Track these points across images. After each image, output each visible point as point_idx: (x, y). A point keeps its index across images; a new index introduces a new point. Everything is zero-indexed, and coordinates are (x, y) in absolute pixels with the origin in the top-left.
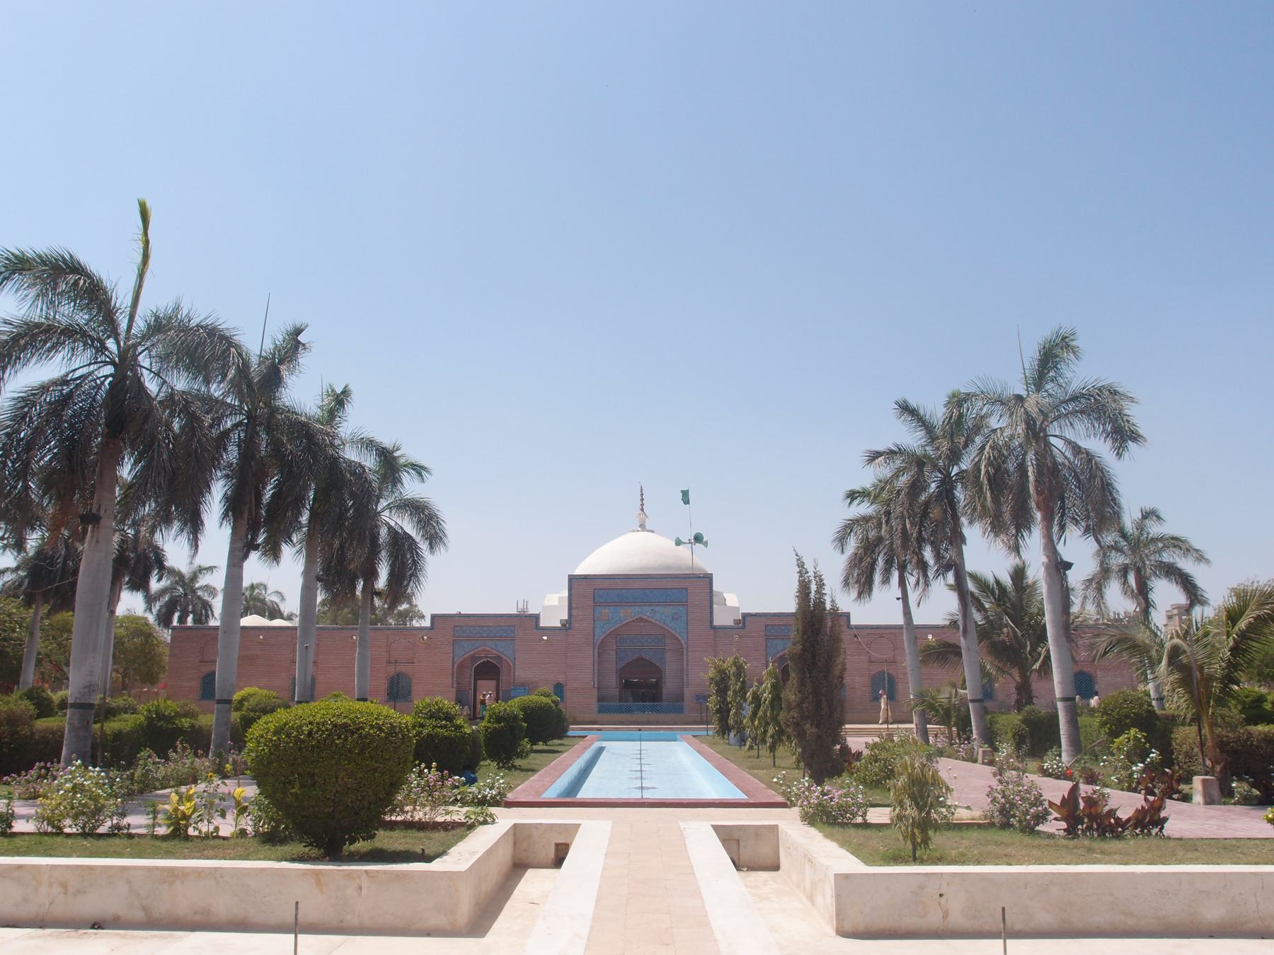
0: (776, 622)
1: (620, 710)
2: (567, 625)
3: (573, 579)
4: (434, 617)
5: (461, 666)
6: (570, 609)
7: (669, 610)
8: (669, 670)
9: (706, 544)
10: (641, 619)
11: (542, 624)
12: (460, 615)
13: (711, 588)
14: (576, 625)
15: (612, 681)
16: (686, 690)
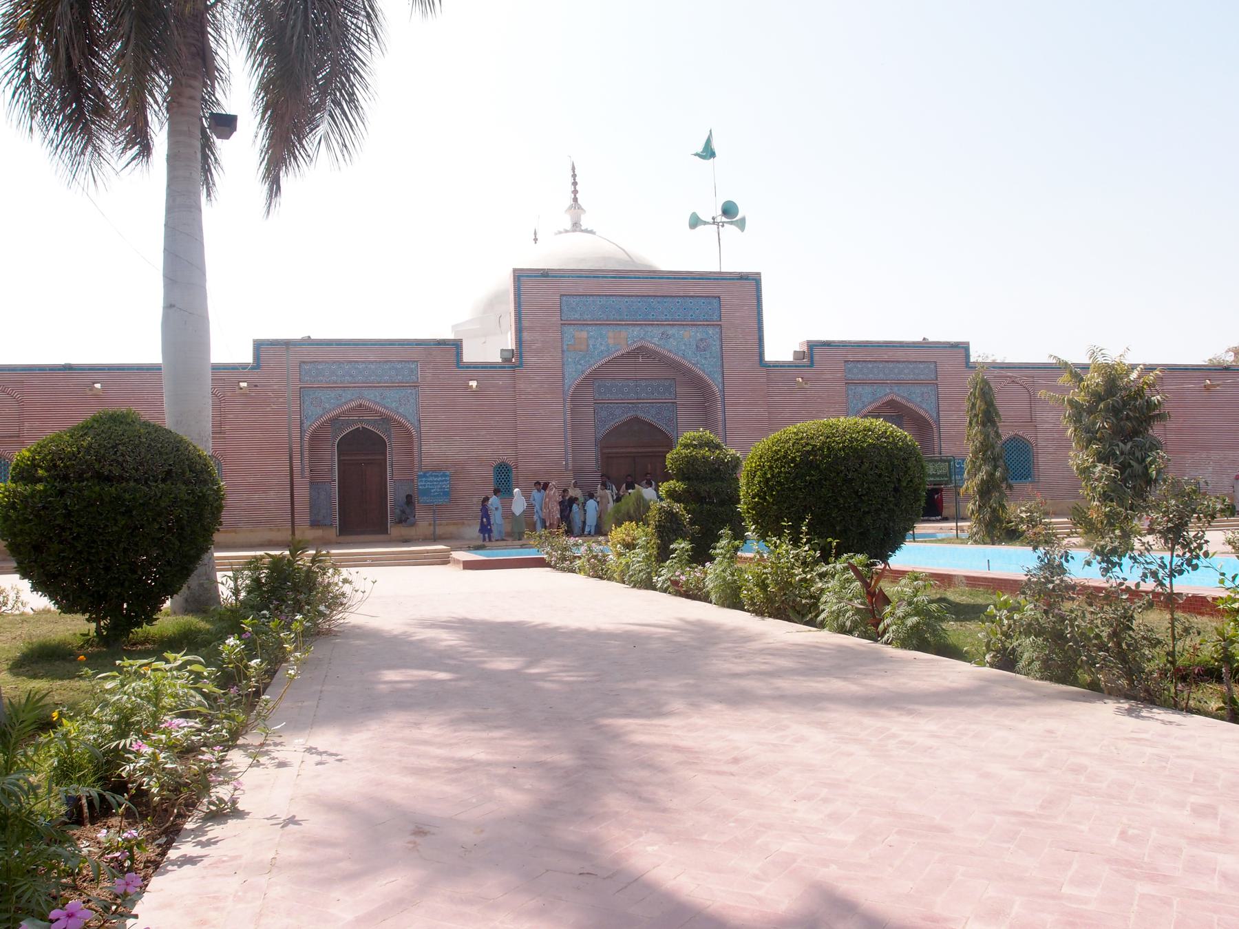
2: (513, 361)
3: (520, 276)
5: (315, 438)
6: (519, 331)
9: (741, 224)
10: (641, 352)
11: (469, 356)
12: (308, 342)
14: (530, 359)
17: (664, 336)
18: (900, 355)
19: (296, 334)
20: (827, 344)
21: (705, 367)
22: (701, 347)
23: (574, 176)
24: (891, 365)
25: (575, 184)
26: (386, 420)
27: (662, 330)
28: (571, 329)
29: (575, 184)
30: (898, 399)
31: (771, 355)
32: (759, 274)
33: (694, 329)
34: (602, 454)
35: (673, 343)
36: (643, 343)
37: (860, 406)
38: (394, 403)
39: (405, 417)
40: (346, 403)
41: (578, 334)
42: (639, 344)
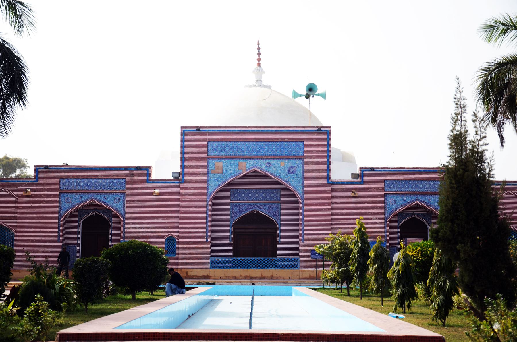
0: (396, 176)
1: (235, 265)
2: (179, 178)
3: (185, 131)
4: (38, 169)
5: (68, 219)
6: (183, 161)
7: (287, 163)
8: (284, 223)
9: (323, 96)
10: (256, 174)
11: (154, 176)
12: (66, 167)
13: (329, 143)
14: (188, 178)
15: (226, 235)
16: (302, 246)
17: (269, 165)
18: (424, 176)
19: (58, 162)
20: (372, 169)
21: (294, 183)
22: (291, 171)
23: (259, 49)
24: (418, 183)
25: (259, 54)
26: (108, 212)
27: (267, 161)
28: (213, 161)
29: (259, 54)
30: (422, 204)
31: (335, 176)
32: (329, 127)
33: (287, 161)
34: (234, 232)
35: (273, 170)
36: (255, 169)
37: (394, 207)
38: (110, 201)
39: (117, 210)
40: (84, 201)
41: (217, 164)
42: (253, 170)
